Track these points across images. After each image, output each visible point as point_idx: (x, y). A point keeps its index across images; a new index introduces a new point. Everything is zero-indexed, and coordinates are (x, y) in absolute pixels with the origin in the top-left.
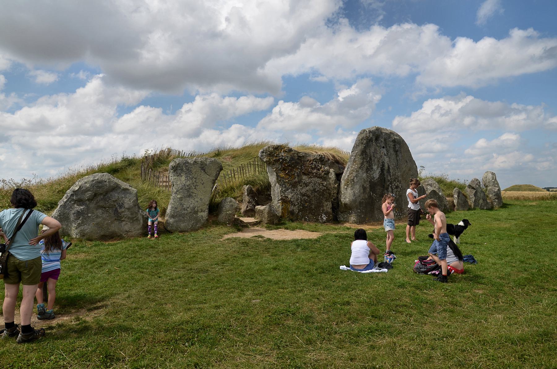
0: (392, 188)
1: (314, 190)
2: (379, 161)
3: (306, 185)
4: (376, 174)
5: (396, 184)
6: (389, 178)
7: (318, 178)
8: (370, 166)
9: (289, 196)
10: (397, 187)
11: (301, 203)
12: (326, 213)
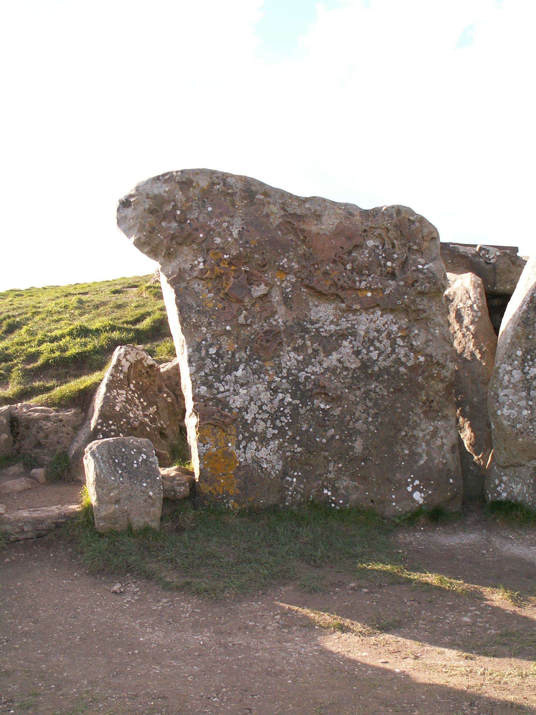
1: (365, 366)
7: (384, 311)
9: (237, 402)
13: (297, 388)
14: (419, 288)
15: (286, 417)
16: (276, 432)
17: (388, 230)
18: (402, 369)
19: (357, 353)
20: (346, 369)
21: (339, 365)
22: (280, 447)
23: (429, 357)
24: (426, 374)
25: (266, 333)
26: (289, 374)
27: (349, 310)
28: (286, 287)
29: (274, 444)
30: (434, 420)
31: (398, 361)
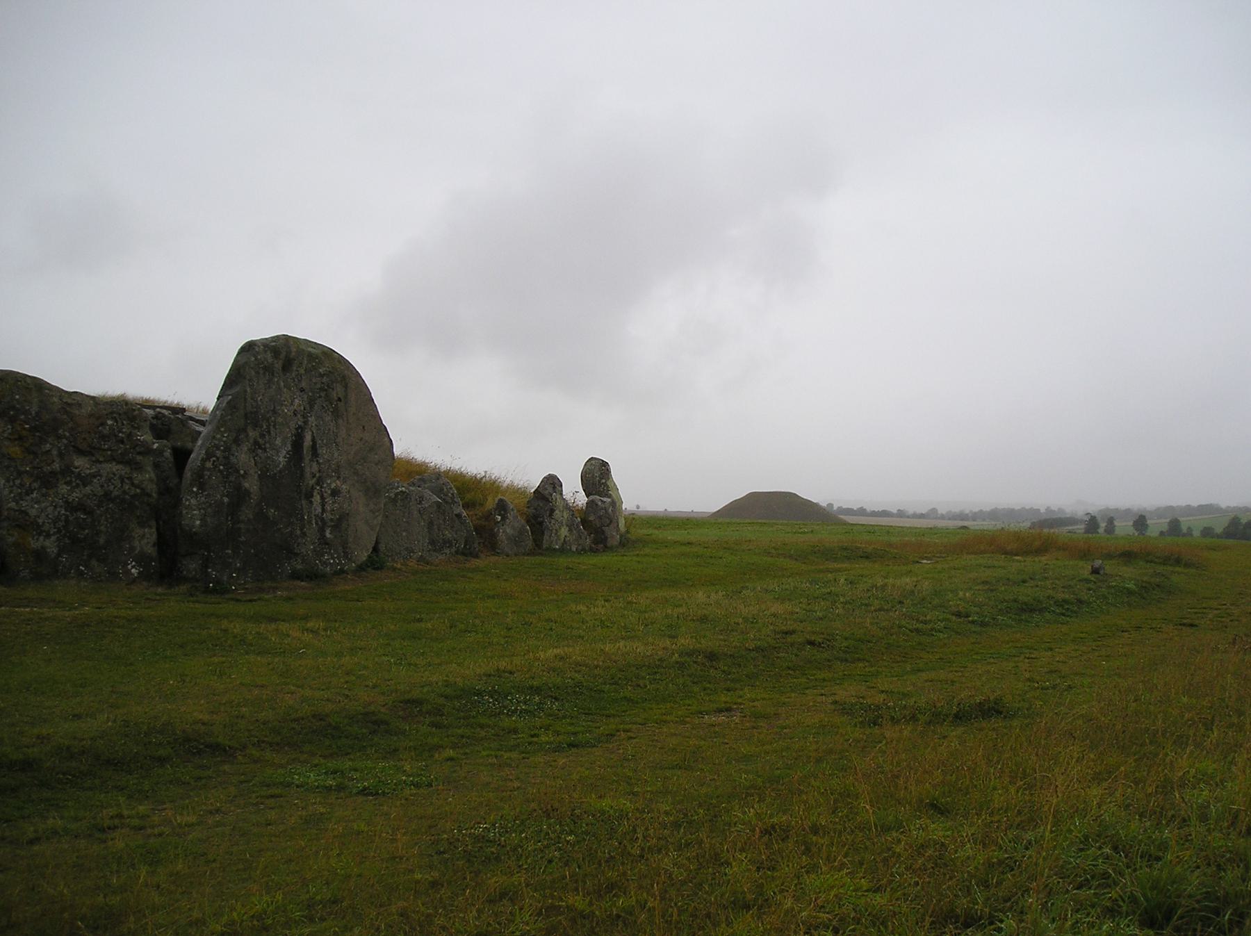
0: (322, 498)
1: (107, 495)
3: (85, 480)
5: (333, 486)
8: (262, 436)
9: (33, 512)
10: (335, 493)
12: (142, 560)
13: (69, 505)
19: (102, 486)
29: (53, 538)
31: (124, 492)
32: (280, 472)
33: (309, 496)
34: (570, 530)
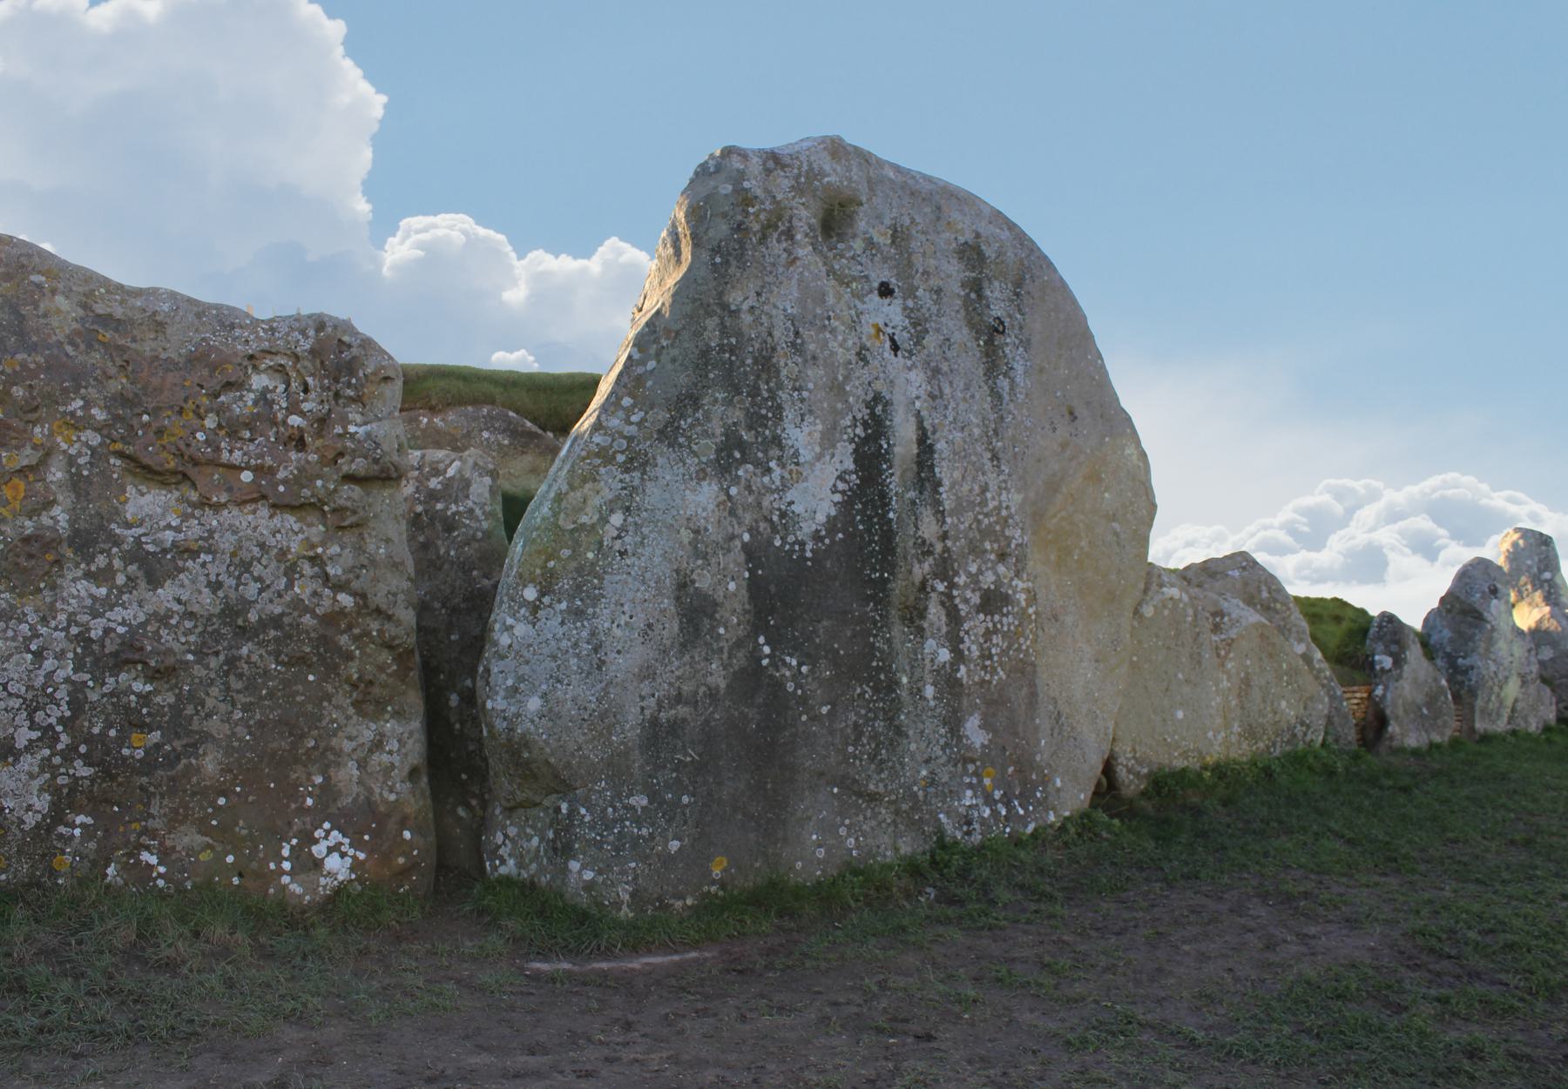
0: (954, 617)
1: (232, 611)
2: (837, 389)
3: (154, 567)
4: (815, 495)
5: (988, 580)
6: (929, 529)
8: (755, 421)
10: (993, 601)
11: (81, 736)
12: (363, 822)
14: (345, 468)
15: (58, 706)
16: (35, 735)
17: (297, 358)
18: (307, 620)
19: (215, 586)
20: (191, 615)
21: (176, 607)
22: (46, 765)
23: (361, 596)
24: (356, 631)
25: (27, 540)
26: (71, 620)
27: (204, 503)
28: (79, 454)
30: (375, 719)
31: (297, 603)
32: (817, 537)
33: (914, 615)
34: (1524, 683)
